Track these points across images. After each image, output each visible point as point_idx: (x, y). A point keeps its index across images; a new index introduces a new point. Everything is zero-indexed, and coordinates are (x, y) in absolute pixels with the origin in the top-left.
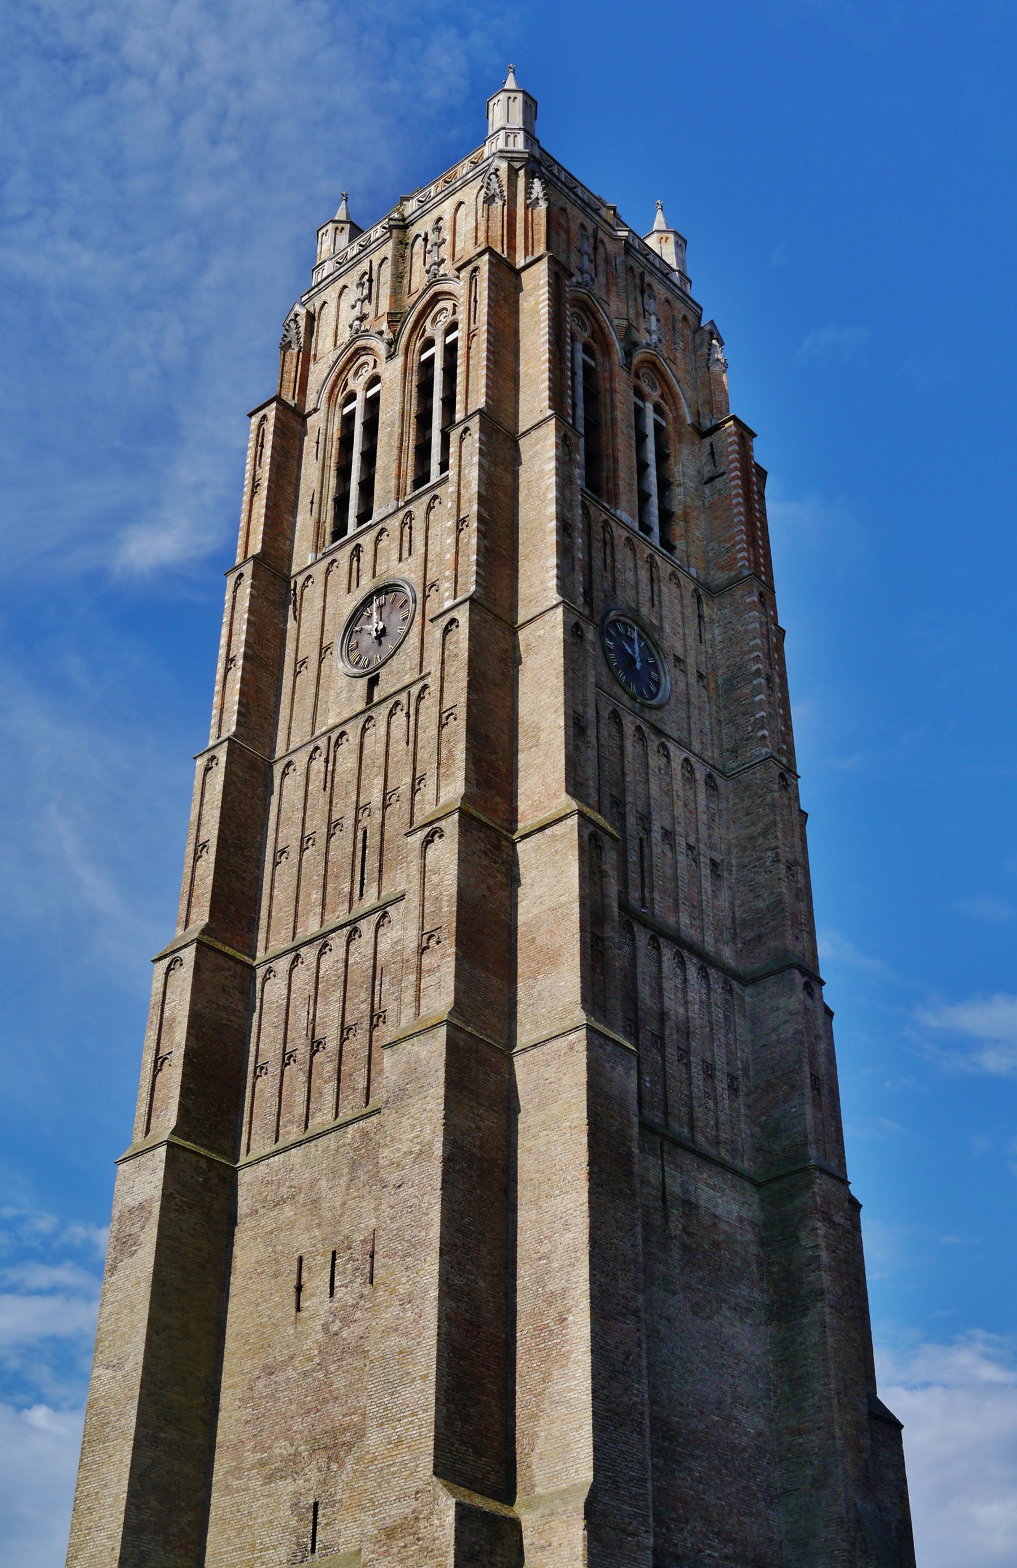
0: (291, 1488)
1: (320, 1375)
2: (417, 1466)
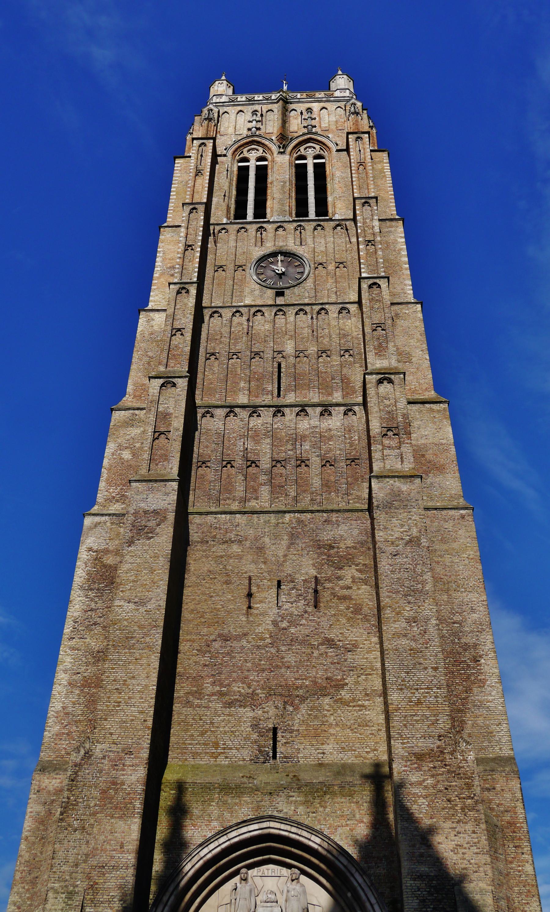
0: (251, 714)
1: (273, 650)
2: (438, 720)
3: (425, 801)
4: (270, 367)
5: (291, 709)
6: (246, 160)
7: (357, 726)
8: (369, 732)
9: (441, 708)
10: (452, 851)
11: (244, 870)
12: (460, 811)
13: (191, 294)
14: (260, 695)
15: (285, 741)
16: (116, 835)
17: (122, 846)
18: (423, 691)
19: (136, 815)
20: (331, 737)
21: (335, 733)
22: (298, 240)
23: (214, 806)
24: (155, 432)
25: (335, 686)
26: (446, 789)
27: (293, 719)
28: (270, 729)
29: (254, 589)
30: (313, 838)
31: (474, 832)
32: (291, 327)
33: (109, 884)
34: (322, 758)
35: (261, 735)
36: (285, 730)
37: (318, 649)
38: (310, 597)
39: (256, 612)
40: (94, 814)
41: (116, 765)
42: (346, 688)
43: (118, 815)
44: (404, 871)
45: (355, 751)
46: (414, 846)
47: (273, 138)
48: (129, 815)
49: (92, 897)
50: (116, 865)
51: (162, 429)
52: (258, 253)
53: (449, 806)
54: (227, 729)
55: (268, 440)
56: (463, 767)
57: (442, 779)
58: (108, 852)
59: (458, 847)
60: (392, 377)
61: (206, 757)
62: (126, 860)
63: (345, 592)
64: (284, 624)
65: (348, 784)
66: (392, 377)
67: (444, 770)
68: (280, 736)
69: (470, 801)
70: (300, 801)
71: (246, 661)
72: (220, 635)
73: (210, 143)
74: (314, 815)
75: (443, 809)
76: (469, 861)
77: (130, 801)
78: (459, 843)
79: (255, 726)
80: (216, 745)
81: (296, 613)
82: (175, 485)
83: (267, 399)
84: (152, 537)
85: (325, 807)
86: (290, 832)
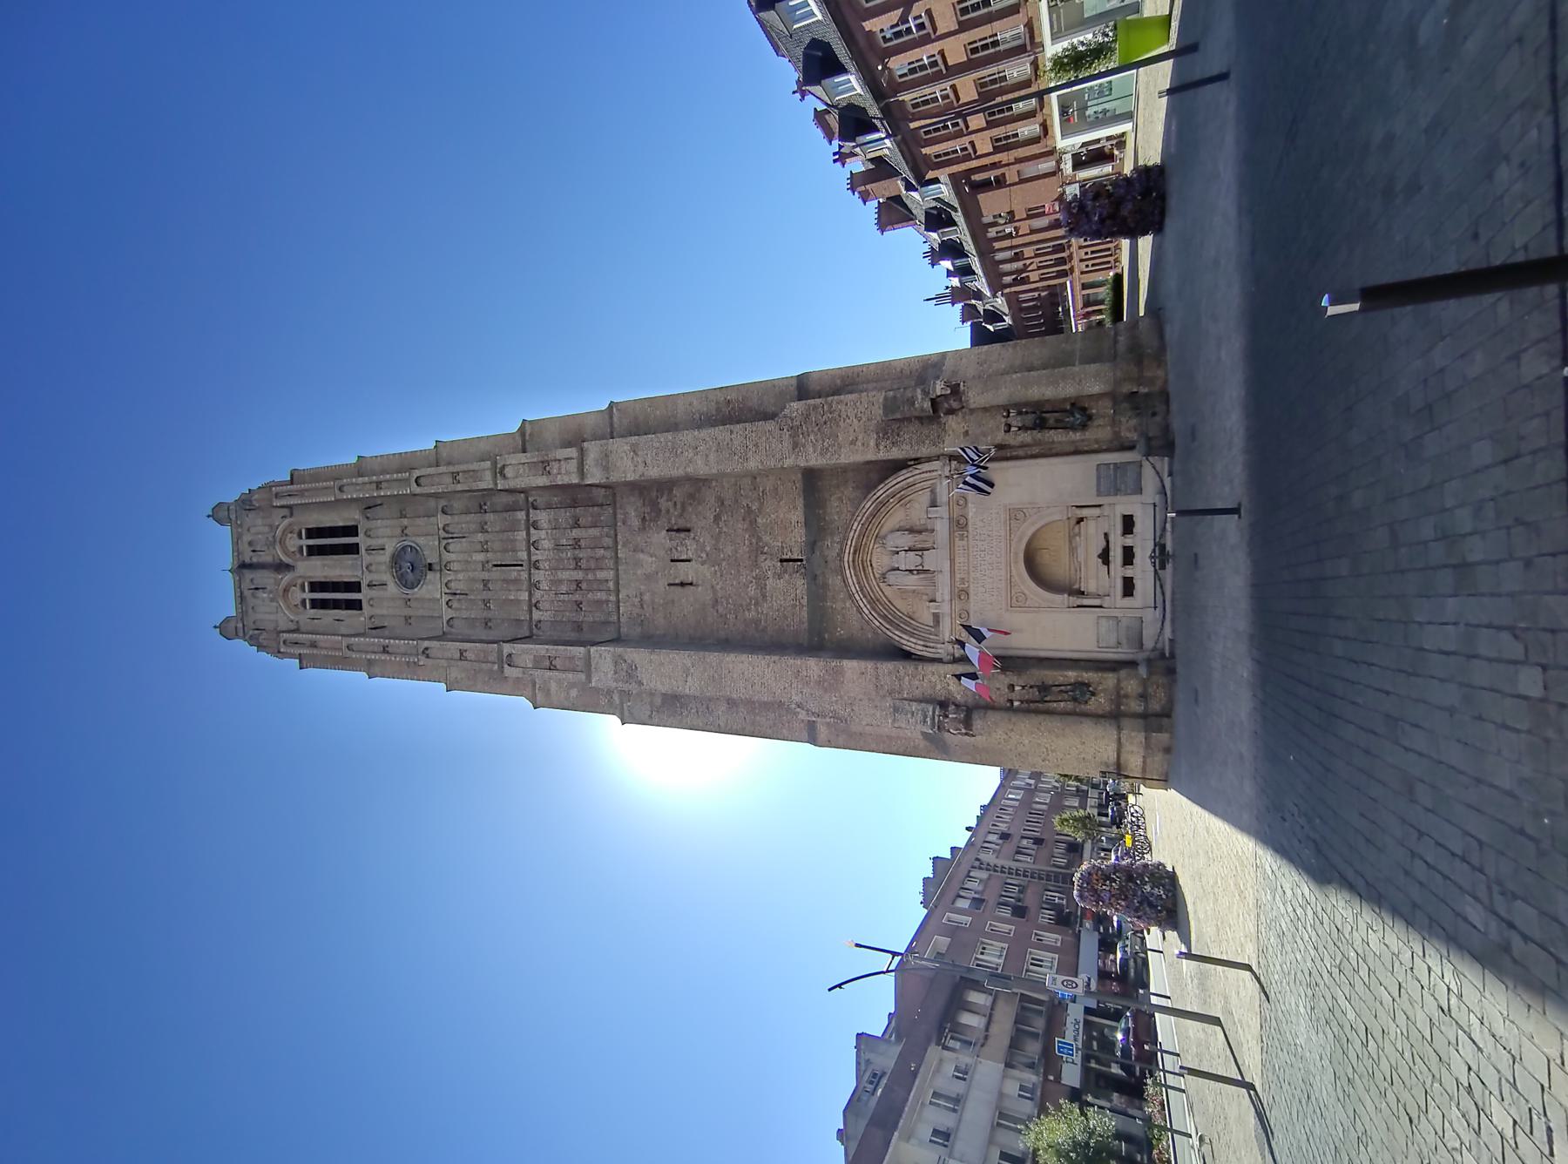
1: (724, 564)
4: (496, 574)
5: (766, 548)
6: (304, 601)
13: (429, 646)
17: (863, 673)
22: (381, 552)
24: (550, 669)
29: (677, 581)
30: (854, 528)
31: (847, 404)
32: (461, 557)
35: (786, 572)
37: (721, 528)
38: (682, 535)
39: (695, 579)
40: (841, 697)
42: (750, 505)
47: (280, 577)
51: (548, 663)
52: (393, 588)
55: (559, 573)
60: (499, 466)
63: (679, 506)
64: (704, 555)
66: (499, 466)
71: (733, 585)
72: (713, 608)
73: (285, 636)
80: (794, 606)
81: (695, 546)
82: (593, 649)
83: (525, 575)
84: (635, 666)
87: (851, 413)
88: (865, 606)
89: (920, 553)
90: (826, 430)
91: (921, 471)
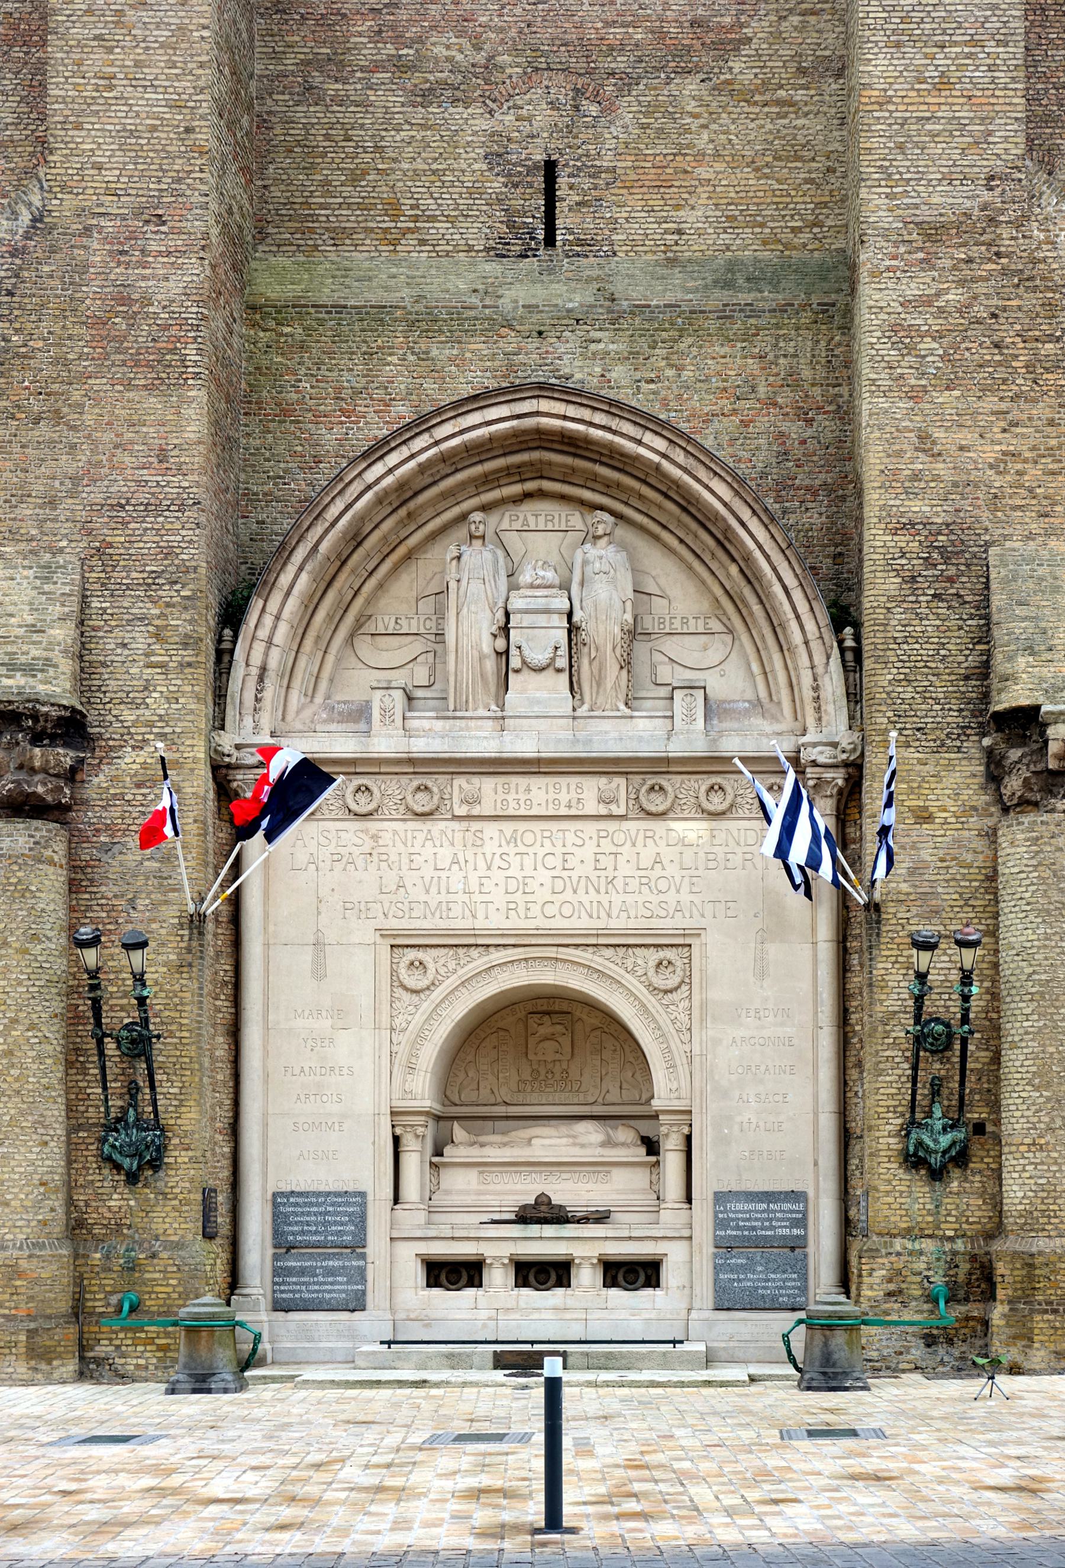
0: (483, 124)
2: (990, 133)
3: (936, 345)
5: (594, 109)
7: (770, 159)
8: (802, 176)
9: (1001, 101)
10: (991, 466)
11: (477, 516)
12: (1024, 370)
14: (508, 71)
15: (577, 198)
16: (145, 429)
17: (162, 457)
18: (958, 50)
19: (190, 382)
20: (700, 190)
21: (712, 176)
23: (395, 365)
25: (715, 45)
26: (994, 316)
27: (598, 138)
28: (536, 167)
30: (648, 438)
31: (1051, 423)
33: (141, 545)
34: (677, 244)
36: (579, 169)
41: (122, 253)
43: (142, 382)
44: (871, 512)
45: (762, 225)
46: (899, 454)
48: (173, 381)
49: (103, 575)
50: (152, 501)
53: (998, 358)
54: (420, 165)
56: (1044, 260)
57: (985, 291)
58: (129, 471)
59: (1008, 458)
61: (368, 242)
62: (176, 490)
65: (741, 311)
67: (994, 266)
68: (563, 186)
69: (1051, 346)
70: (617, 353)
74: (652, 386)
75: (981, 366)
76: (1030, 492)
77: (171, 346)
78: (1012, 448)
79: (495, 158)
80: (393, 209)
85: (680, 369)
86: (591, 424)
87: (1021, 442)
88: (390, 471)
89: (562, 662)
90: (976, 350)
91: (820, 670)
